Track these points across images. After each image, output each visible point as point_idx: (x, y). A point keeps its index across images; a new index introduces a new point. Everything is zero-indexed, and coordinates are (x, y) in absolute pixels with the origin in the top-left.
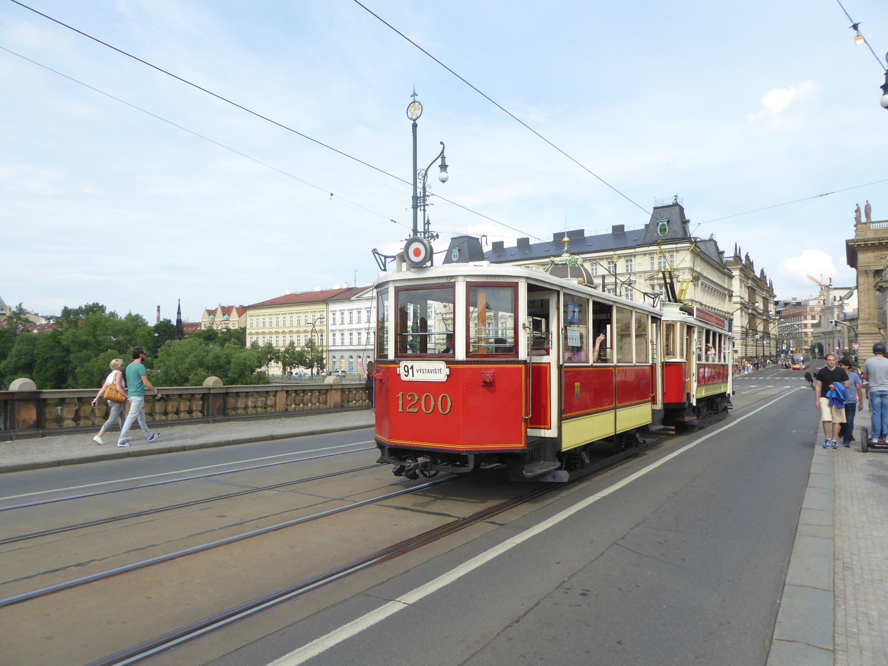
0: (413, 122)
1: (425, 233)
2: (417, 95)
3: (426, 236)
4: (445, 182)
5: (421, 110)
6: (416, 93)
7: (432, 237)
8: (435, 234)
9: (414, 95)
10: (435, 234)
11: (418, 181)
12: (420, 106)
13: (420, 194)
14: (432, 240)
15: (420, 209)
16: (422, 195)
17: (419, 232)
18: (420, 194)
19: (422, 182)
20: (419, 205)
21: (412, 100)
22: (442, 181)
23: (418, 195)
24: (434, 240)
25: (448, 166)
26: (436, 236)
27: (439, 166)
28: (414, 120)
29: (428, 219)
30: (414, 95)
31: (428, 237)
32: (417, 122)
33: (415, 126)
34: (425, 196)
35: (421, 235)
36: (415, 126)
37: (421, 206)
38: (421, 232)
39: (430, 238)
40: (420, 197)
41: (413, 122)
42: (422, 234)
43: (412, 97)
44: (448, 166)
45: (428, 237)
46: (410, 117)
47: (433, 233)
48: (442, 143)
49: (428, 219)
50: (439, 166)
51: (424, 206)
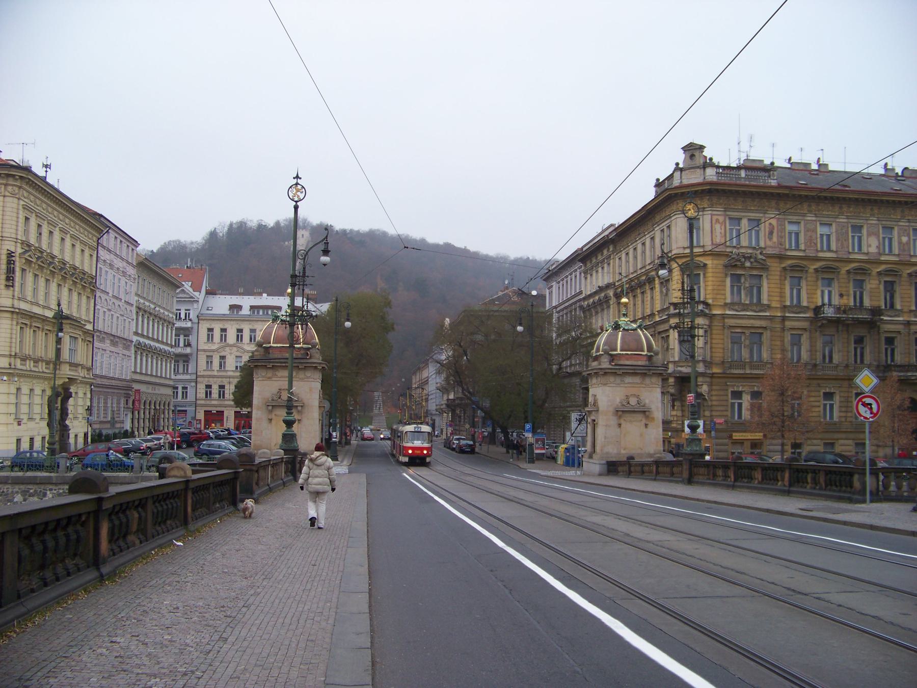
0: (295, 203)
2: (300, 178)
6: (300, 176)
9: (297, 177)
16: (301, 274)
21: (295, 181)
28: (296, 202)
30: (297, 177)
32: (298, 203)
33: (296, 208)
34: (304, 275)
36: (296, 208)
37: (299, 285)
40: (299, 276)
43: (294, 178)
46: (291, 197)
51: (303, 285)
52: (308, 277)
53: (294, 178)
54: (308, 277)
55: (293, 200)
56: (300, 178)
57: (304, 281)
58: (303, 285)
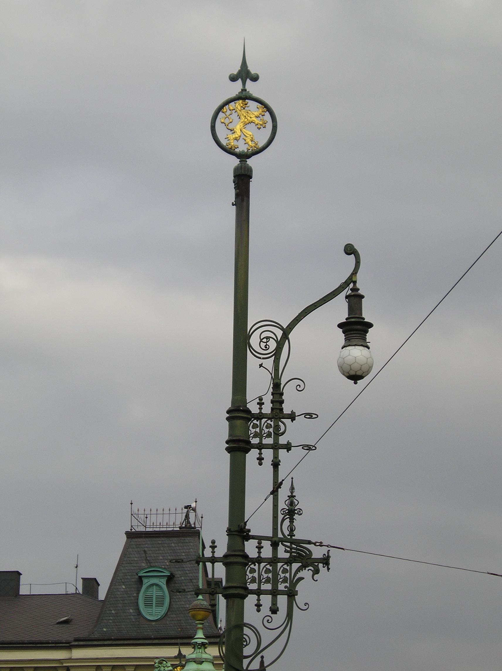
0: (235, 162)
2: (255, 79)
3: (282, 553)
4: (361, 377)
5: (270, 125)
6: (253, 69)
10: (317, 553)
11: (252, 361)
12: (267, 114)
13: (261, 404)
14: (306, 573)
15: (260, 459)
16: (267, 409)
17: (254, 537)
18: (261, 404)
19: (269, 363)
20: (255, 441)
21: (236, 87)
22: (350, 377)
23: (254, 408)
24: (316, 571)
25: (370, 325)
27: (340, 326)
29: (292, 497)
31: (289, 562)
32: (250, 162)
35: (260, 548)
38: (260, 539)
39: (295, 566)
40: (260, 416)
41: (235, 162)
42: (267, 545)
43: (233, 79)
44: (370, 325)
45: (289, 562)
47: (310, 547)
48: (350, 250)
49: (292, 497)
50: (340, 326)
51: (276, 447)
52: (292, 417)
53: (233, 79)
54: (292, 417)
55: (230, 151)
56: (255, 79)
57: (278, 434)
58: (276, 447)
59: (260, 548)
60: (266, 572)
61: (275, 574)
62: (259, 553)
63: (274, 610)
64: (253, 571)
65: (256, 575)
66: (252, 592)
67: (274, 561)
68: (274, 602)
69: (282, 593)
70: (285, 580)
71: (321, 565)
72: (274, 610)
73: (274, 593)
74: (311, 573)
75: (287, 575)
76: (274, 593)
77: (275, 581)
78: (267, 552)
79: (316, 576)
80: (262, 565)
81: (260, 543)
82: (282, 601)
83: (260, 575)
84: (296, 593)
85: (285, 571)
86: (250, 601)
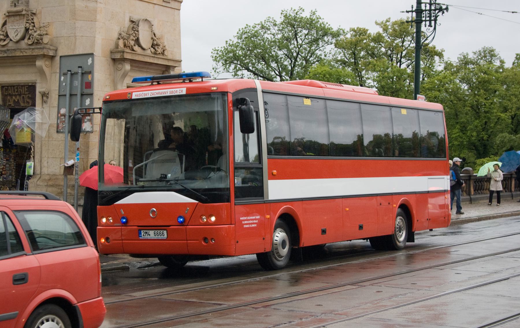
1: (431, 4)
7: (441, 9)
8: (444, 7)
10: (444, 7)
14: (440, 13)
24: (443, 13)
26: (445, 9)
31: (435, 10)
35: (426, 6)
38: (426, 3)
39: (437, 11)
42: (428, 6)
45: (435, 10)
47: (441, 5)
59: (426, 6)
60: (428, 14)
61: (430, 14)
62: (426, 8)
63: (430, 26)
64: (423, 14)
65: (424, 15)
66: (424, 21)
67: (430, 10)
68: (430, 23)
69: (433, 20)
70: (433, 16)
71: (445, 11)
72: (430, 26)
73: (430, 21)
74: (442, 13)
75: (434, 14)
76: (430, 21)
77: (430, 17)
78: (428, 8)
79: (443, 14)
80: (427, 12)
81: (426, 5)
82: (433, 23)
83: (426, 15)
84: (437, 20)
85: (433, 13)
86: (424, 23)
